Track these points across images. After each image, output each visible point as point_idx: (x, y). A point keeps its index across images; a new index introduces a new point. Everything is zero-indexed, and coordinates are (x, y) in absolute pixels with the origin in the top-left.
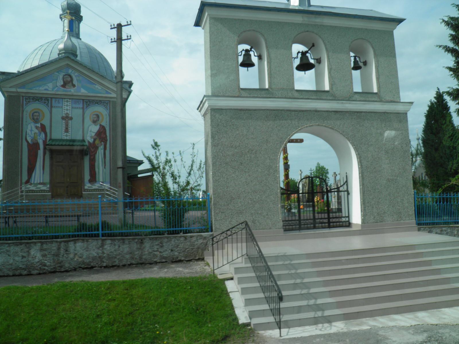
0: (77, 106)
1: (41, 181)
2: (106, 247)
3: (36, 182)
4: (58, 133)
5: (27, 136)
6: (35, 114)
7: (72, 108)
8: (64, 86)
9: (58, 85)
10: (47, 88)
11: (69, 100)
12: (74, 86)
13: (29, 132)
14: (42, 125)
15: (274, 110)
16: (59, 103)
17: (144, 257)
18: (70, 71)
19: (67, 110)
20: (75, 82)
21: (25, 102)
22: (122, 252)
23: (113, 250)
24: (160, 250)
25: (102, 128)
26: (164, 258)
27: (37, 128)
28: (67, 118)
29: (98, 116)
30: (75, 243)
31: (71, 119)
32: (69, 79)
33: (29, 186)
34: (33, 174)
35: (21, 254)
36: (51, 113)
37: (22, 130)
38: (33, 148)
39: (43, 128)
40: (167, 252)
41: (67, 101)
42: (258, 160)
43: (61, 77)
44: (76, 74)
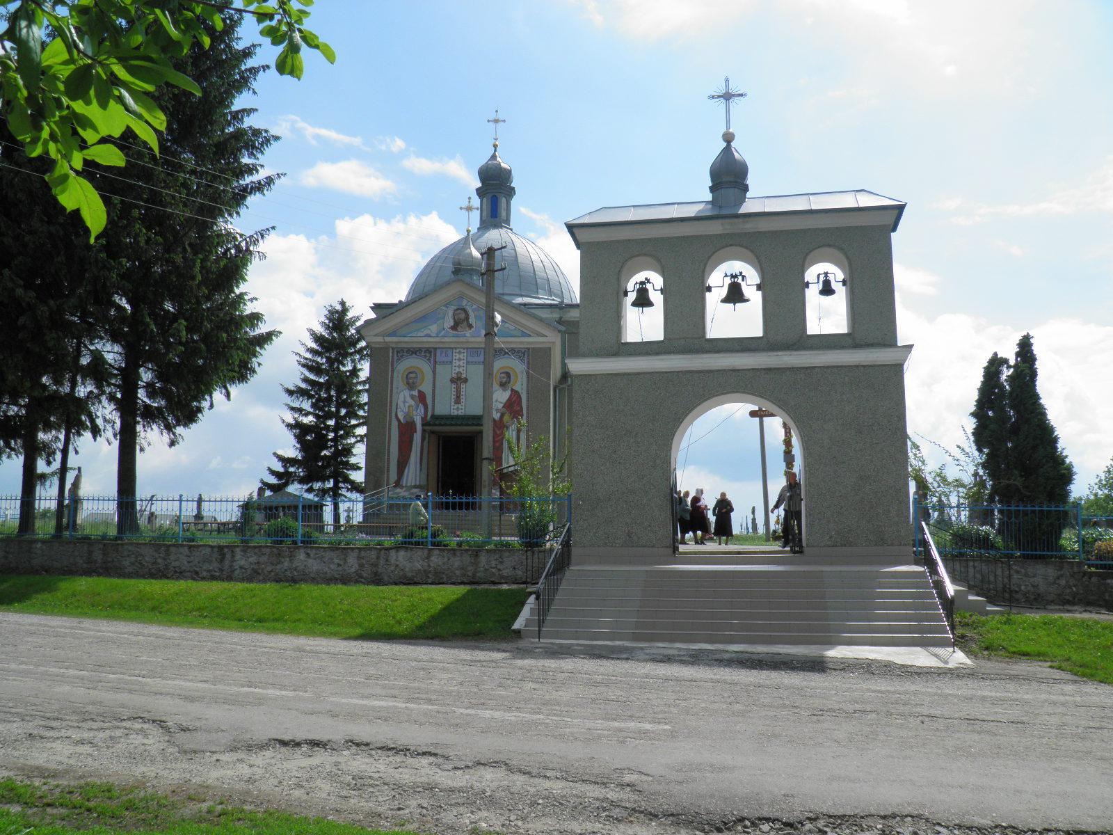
0: (475, 359)
1: (418, 483)
2: (432, 558)
3: (409, 485)
4: (445, 406)
5: (399, 410)
6: (411, 375)
7: (468, 363)
8: (454, 328)
9: (445, 327)
10: (429, 332)
11: (462, 350)
12: (470, 326)
13: (401, 404)
14: (419, 391)
15: (666, 372)
16: (447, 355)
17: (478, 575)
18: (464, 303)
19: (459, 366)
20: (472, 320)
21: (396, 358)
22: (452, 566)
23: (440, 563)
24: (498, 567)
25: (515, 393)
26: (503, 577)
27: (412, 397)
28: (458, 380)
29: (508, 375)
30: (397, 551)
31: (466, 380)
32: (463, 316)
33: (398, 490)
34: (406, 471)
35: (336, 561)
36: (434, 372)
37: (391, 402)
38: (407, 429)
39: (422, 398)
40: (507, 571)
41: (460, 353)
42: (639, 447)
43: (450, 313)
44: (474, 307)
